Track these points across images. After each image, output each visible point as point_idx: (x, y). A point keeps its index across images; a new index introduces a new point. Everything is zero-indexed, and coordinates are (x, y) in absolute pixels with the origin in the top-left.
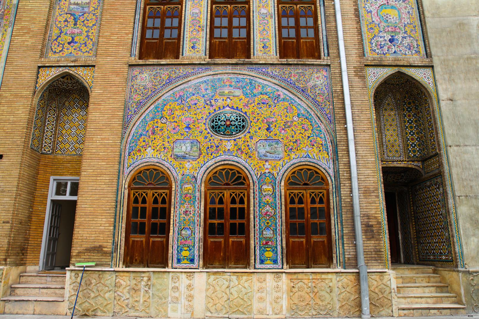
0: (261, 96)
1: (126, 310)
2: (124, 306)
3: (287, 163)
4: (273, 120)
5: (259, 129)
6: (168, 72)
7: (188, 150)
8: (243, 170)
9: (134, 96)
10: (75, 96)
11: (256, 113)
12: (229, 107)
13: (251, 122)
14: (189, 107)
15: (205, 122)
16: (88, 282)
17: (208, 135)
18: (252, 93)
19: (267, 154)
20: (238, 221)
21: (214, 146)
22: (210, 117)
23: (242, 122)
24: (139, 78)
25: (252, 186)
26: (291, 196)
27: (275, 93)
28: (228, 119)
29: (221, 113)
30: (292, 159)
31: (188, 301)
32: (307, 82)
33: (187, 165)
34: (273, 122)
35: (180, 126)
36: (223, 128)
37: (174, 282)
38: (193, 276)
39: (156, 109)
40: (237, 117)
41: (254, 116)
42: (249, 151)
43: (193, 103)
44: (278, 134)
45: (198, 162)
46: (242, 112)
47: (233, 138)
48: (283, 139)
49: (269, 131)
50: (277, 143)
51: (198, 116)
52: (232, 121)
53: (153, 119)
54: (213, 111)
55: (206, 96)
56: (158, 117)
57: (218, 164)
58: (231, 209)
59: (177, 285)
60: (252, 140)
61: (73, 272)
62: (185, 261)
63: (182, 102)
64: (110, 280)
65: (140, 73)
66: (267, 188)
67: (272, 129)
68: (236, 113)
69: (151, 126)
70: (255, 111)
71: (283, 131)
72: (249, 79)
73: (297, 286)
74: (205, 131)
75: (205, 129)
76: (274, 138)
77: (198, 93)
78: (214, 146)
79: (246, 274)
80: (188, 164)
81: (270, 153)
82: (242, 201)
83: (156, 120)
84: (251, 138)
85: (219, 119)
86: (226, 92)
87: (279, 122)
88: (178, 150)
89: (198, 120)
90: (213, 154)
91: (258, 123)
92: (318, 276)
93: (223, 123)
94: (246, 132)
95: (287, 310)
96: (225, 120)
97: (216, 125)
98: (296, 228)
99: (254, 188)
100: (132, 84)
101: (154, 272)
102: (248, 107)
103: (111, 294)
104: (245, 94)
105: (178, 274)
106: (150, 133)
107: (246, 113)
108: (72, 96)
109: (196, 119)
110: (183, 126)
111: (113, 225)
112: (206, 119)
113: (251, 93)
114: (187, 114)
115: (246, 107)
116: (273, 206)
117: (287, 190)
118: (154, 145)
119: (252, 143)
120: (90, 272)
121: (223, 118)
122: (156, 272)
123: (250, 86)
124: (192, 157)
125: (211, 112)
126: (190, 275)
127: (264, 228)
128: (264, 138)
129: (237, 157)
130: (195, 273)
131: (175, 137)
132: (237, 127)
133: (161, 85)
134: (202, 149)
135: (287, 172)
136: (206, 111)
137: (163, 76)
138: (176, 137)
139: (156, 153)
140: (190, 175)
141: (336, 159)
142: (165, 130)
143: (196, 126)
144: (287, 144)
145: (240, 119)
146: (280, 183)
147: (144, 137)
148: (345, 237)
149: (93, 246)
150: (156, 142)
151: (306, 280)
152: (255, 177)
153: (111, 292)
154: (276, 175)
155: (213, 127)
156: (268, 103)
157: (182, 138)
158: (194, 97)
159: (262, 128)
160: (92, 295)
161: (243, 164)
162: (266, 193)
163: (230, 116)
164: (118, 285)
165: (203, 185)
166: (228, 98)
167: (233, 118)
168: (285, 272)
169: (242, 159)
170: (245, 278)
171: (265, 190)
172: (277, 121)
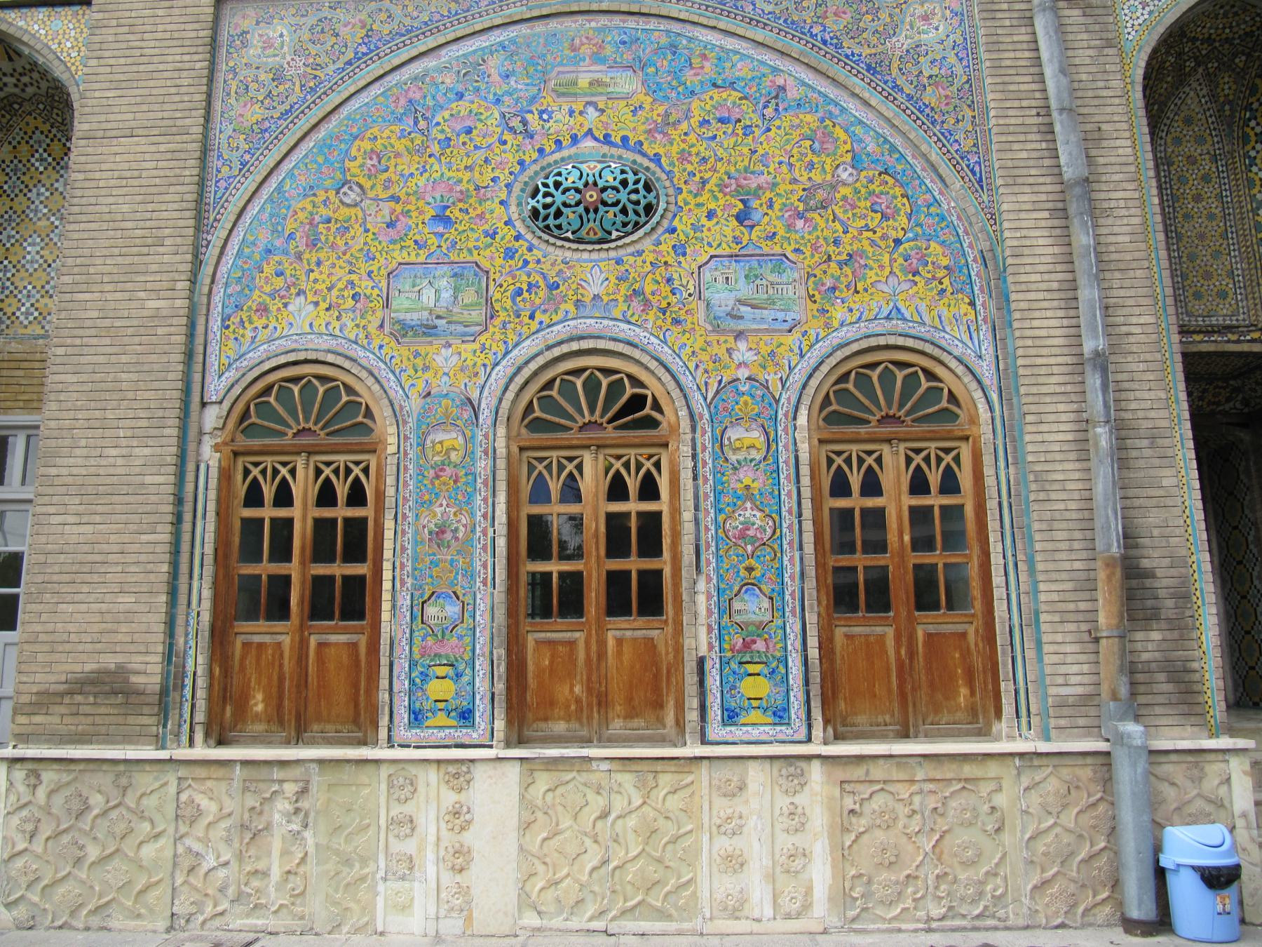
0: (714, 93)
1: (220, 909)
2: (210, 892)
3: (817, 341)
4: (762, 180)
5: (711, 215)
6: (363, 16)
7: (443, 303)
8: (652, 373)
10: (33, 123)
11: (694, 159)
12: (596, 139)
13: (680, 191)
14: (444, 144)
15: (503, 196)
16: (76, 805)
17: (517, 244)
18: (681, 84)
19: (743, 309)
21: (541, 283)
22: (524, 178)
23: (642, 192)
24: (255, 39)
25: (688, 430)
26: (834, 467)
27: (766, 82)
28: (591, 180)
29: (563, 159)
30: (836, 324)
31: (453, 868)
32: (891, 31)
33: (444, 358)
34: (759, 187)
35: (414, 214)
36: (572, 216)
37: (398, 800)
38: (468, 777)
39: (320, 152)
40: (623, 172)
41: (690, 168)
42: (673, 299)
43: (458, 127)
44: (781, 232)
45: (483, 348)
46: (644, 155)
47: (612, 254)
48: (797, 250)
49: (746, 223)
50: (778, 269)
51: (477, 174)
52: (604, 190)
53: (310, 191)
54: (535, 155)
55: (506, 98)
56: (328, 183)
57: (557, 352)
58: (610, 517)
59: (408, 809)
60: (682, 259)
61: (18, 766)
62: (441, 719)
63: (416, 123)
64: (155, 796)
65: (258, 23)
66: (746, 436)
67: (756, 216)
68: (620, 157)
70: (694, 150)
71: (800, 224)
72: (668, 31)
73: (867, 808)
74: (506, 230)
75: (506, 223)
76: (766, 250)
77: (477, 90)
78: (541, 283)
79: (671, 766)
81: (753, 307)
82: (649, 490)
84: (680, 250)
85: (557, 185)
86: (583, 82)
87: (782, 189)
88: (407, 304)
89: (477, 188)
90: (539, 316)
91: (706, 196)
92: (948, 771)
93: (572, 197)
94: (660, 230)
95: (830, 899)
96: (580, 185)
97: (546, 206)
98: (856, 585)
99: (693, 440)
100: (231, 64)
101: (321, 762)
102: (665, 134)
103: (162, 849)
104: (653, 89)
105: (413, 770)
106: (300, 243)
107: (657, 159)
108: (22, 125)
109: (472, 188)
110: (422, 213)
111: (164, 588)
112: (507, 186)
113: (674, 83)
114: (436, 167)
115: (659, 137)
116: (769, 504)
117: (821, 441)
118: (317, 286)
119: (682, 272)
120: (82, 767)
121: (571, 179)
122: (331, 761)
123: (670, 57)
124: (460, 329)
125: (528, 160)
126: (459, 773)
127: (736, 588)
128: (728, 251)
129: (629, 323)
130: (478, 765)
131: (396, 254)
132: (624, 211)
133: (340, 65)
134: (498, 296)
135: (819, 376)
136: (510, 156)
137: (344, 32)
140: (451, 395)
141: (1000, 330)
143: (473, 213)
144: (817, 272)
145: (637, 182)
146: (795, 418)
147: (277, 258)
148: (1044, 617)
149: (94, 666)
150: (324, 276)
151: (899, 786)
152: (698, 396)
153: (162, 842)
154: (776, 387)
156: (739, 121)
157: (422, 259)
158: (463, 107)
159: (720, 213)
160: (93, 852)
161: (650, 348)
162: (741, 457)
163: (597, 171)
164: (188, 812)
165: (502, 431)
166: (587, 103)
167: (610, 179)
168: (819, 757)
169: (646, 329)
170: (666, 780)
171: (738, 444)
172: (775, 185)
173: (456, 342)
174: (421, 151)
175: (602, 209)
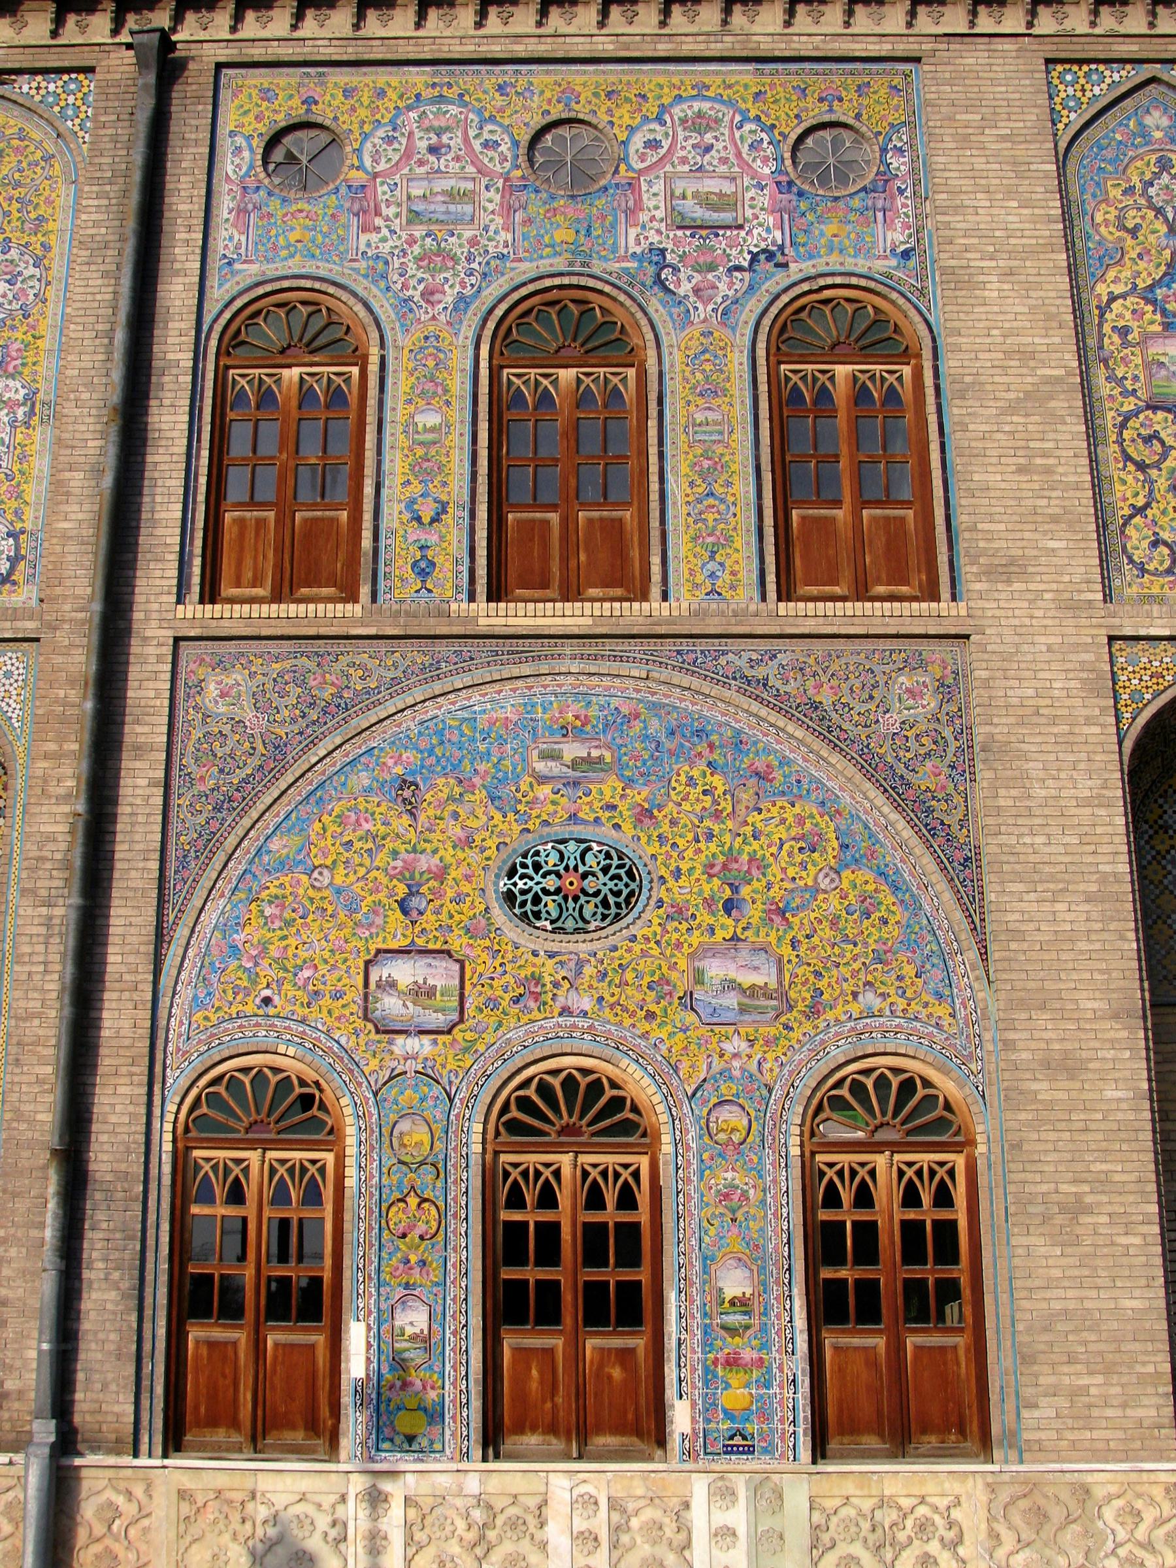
20: (611, 1275)
23: (625, 879)
28: (572, 864)
52: (584, 876)
85: (537, 867)
93: (551, 883)
97: (523, 892)
145: (619, 867)
155: (509, 897)
175: (583, 899)
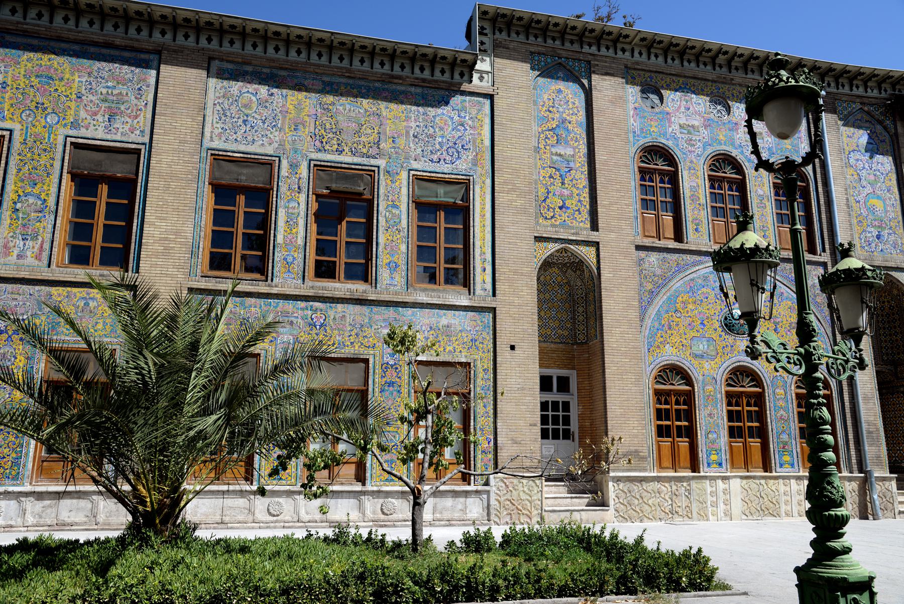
9: (644, 285)
69: (666, 319)
80: (707, 363)
83: (670, 314)
138: (693, 334)
139: (675, 351)
142: (681, 325)
173: (709, 360)
174: (695, 303)
